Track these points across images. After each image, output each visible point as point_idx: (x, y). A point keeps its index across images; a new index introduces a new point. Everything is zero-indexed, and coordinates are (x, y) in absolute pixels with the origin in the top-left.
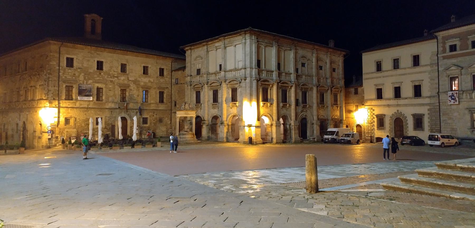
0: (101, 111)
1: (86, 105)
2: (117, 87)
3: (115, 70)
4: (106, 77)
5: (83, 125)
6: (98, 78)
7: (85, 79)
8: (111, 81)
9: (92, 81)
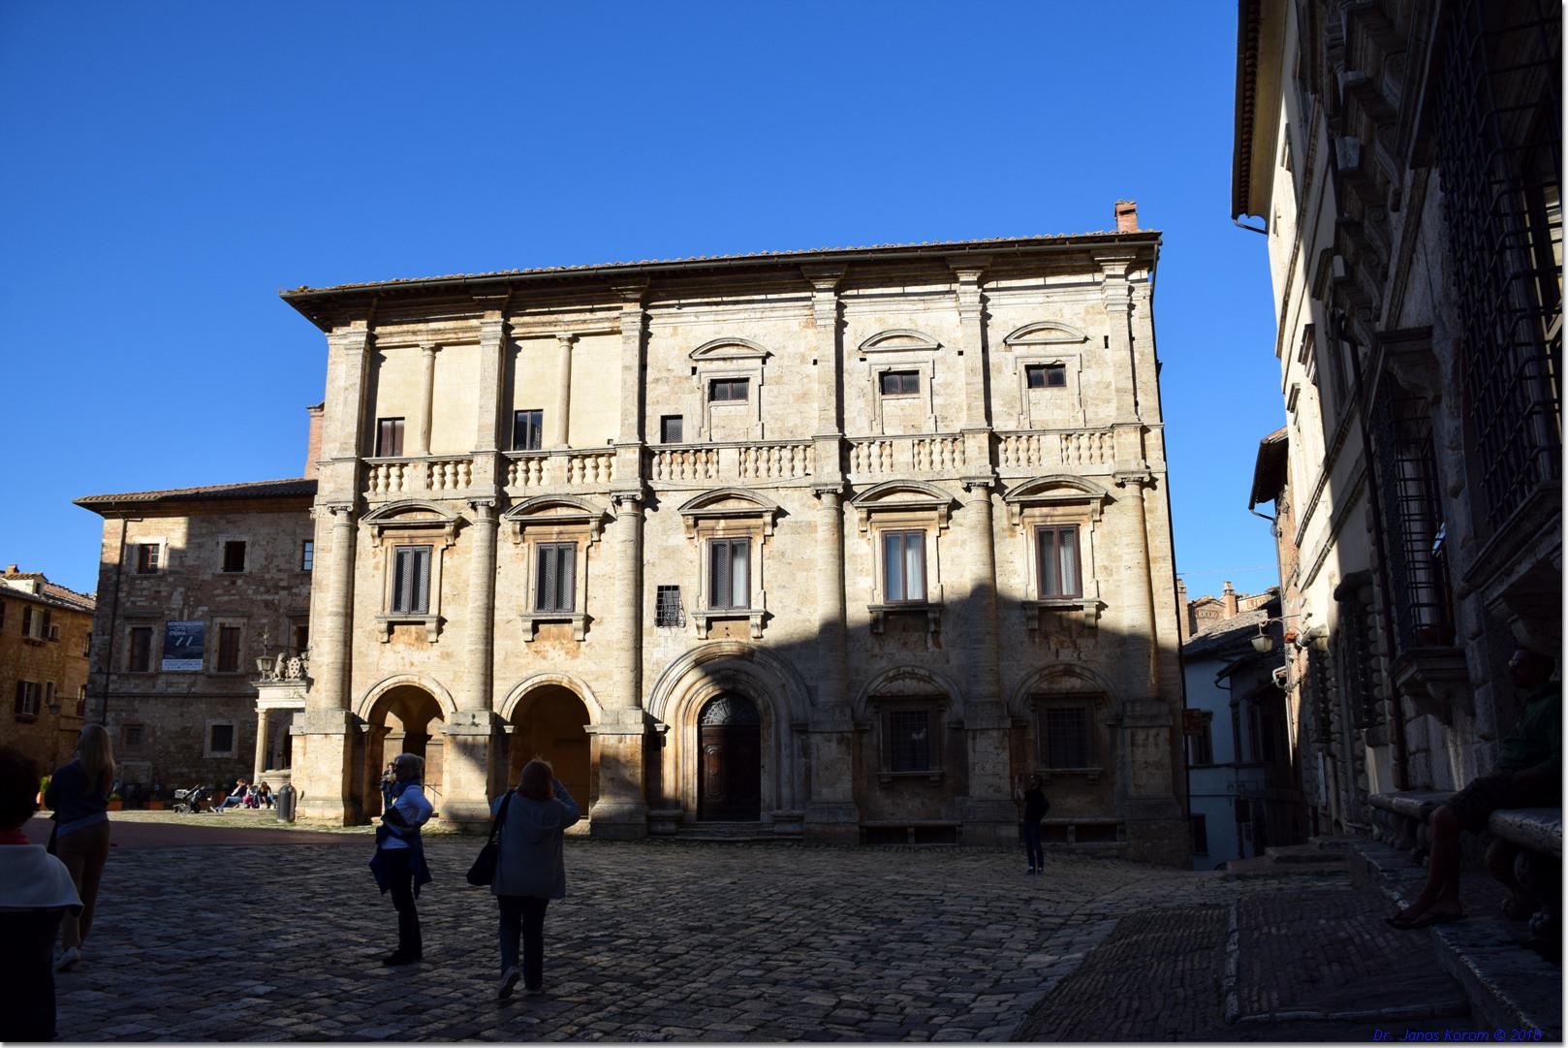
0: (228, 706)
1: (185, 685)
2: (285, 621)
4: (250, 592)
5: (172, 749)
6: (226, 598)
8: (267, 604)
9: (206, 609)
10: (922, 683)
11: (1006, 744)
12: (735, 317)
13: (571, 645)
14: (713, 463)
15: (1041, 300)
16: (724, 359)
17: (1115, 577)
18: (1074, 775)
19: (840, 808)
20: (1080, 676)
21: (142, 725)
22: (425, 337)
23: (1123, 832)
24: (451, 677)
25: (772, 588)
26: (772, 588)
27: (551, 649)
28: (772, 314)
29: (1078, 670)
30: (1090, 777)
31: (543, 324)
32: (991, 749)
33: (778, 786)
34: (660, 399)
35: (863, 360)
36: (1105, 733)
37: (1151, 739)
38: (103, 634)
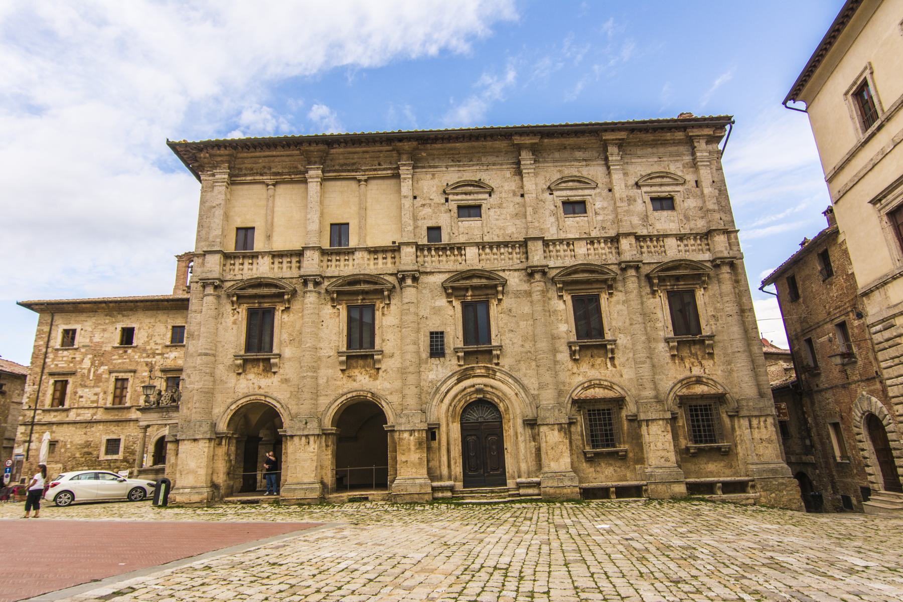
1: (89, 415)
3: (159, 341)
4: (136, 357)
5: (78, 455)
6: (120, 361)
7: (93, 364)
9: (106, 367)
10: (606, 391)
11: (669, 428)
12: (471, 168)
13: (373, 371)
14: (461, 255)
15: (656, 159)
16: (466, 194)
17: (720, 322)
18: (712, 449)
19: (565, 476)
20: (706, 384)
21: (57, 441)
22: (269, 177)
23: (753, 487)
24: (288, 396)
25: (505, 331)
26: (505, 331)
27: (359, 375)
28: (493, 167)
29: (705, 380)
30: (723, 450)
31: (349, 171)
32: (660, 433)
33: (518, 462)
34: (426, 216)
35: (550, 194)
36: (727, 420)
37: (762, 423)
38: (34, 384)
